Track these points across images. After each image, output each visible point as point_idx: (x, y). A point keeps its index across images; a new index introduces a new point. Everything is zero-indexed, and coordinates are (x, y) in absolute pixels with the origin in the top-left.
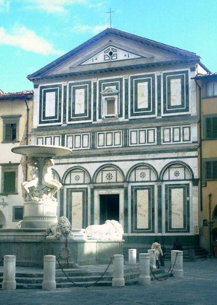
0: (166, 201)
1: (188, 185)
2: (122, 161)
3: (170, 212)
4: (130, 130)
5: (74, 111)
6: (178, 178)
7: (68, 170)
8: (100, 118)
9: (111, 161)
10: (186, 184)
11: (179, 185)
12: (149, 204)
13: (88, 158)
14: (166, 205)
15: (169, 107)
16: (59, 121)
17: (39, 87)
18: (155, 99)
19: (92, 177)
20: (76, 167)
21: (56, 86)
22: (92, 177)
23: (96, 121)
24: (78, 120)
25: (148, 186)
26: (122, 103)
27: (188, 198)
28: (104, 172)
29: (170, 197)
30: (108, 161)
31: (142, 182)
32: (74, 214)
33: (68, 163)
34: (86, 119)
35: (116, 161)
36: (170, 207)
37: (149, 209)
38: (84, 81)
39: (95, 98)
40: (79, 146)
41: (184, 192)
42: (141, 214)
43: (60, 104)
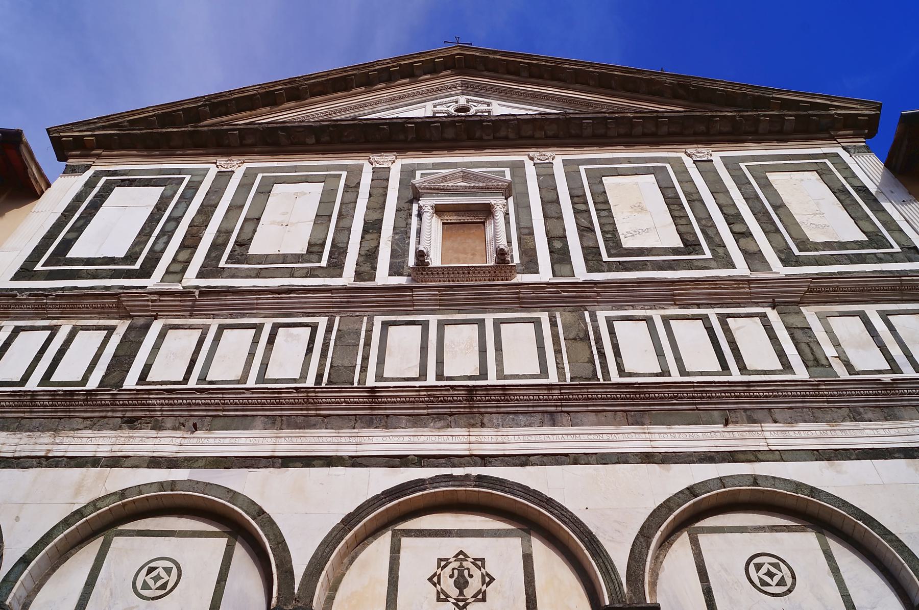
2: (575, 459)
4: (601, 316)
5: (243, 244)
7: (94, 504)
8: (395, 271)
13: (286, 432)
15: (804, 244)
16: (146, 272)
17: (89, 173)
19: (299, 570)
20: (173, 484)
21: (180, 171)
22: (299, 570)
23: (373, 278)
24: (259, 274)
28: (405, 541)
33: (115, 462)
34: (311, 273)
35: (524, 460)
40: (236, 374)
43: (175, 220)
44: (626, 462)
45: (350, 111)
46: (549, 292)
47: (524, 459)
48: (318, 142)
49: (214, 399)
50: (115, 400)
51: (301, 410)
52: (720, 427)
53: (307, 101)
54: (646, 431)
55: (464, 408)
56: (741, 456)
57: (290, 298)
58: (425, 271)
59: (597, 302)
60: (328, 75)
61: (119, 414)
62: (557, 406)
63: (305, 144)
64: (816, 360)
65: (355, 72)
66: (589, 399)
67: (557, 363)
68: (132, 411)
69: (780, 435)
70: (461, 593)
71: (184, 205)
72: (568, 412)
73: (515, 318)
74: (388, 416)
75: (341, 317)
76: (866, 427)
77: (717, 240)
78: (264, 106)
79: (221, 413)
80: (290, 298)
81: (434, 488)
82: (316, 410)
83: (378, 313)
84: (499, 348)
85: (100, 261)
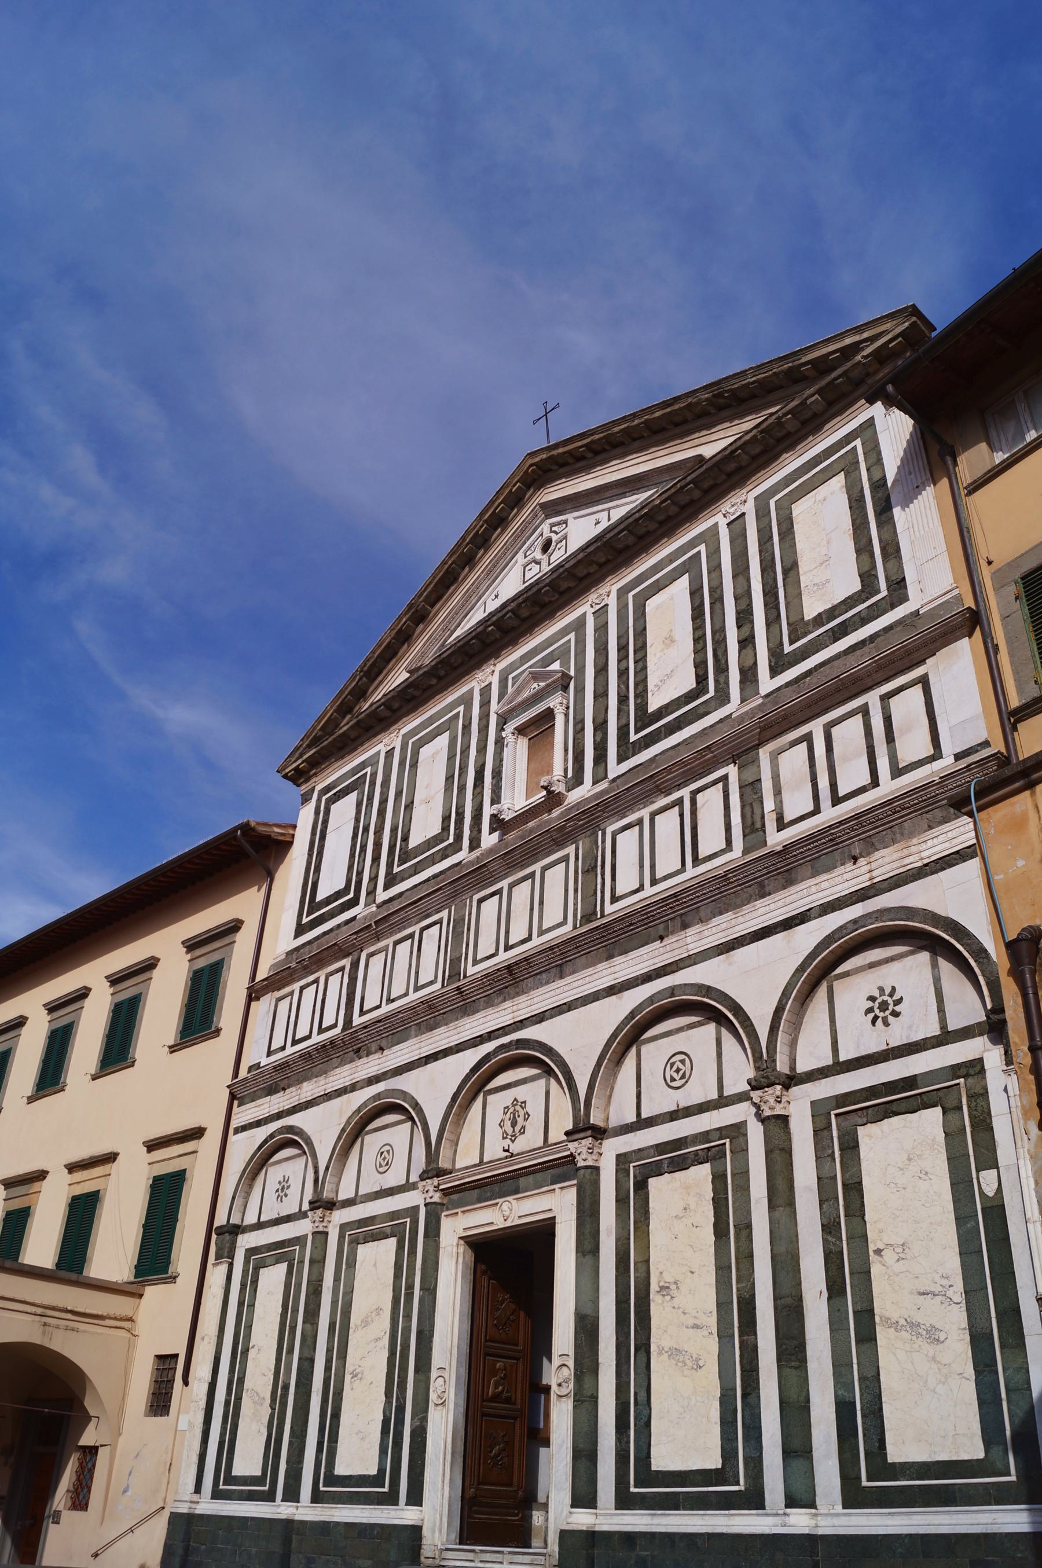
0: (830, 1228)
1: (975, 1068)
3: (866, 1316)
6: (898, 1034)
9: (521, 1024)
10: (955, 1070)
11: (910, 1082)
12: (722, 1269)
14: (832, 1260)
18: (723, 629)
25: (704, 1136)
26: (582, 721)
27: (988, 1181)
29: (855, 1189)
30: (504, 1031)
31: (673, 1116)
32: (354, 1376)
35: (539, 1018)
36: (863, 1275)
37: (723, 1306)
38: (450, 699)
39: (482, 749)
41: (953, 1136)
42: (675, 1353)
44: (598, 1000)
45: (461, 611)
46: (570, 826)
47: (541, 1015)
48: (440, 678)
49: (387, 1023)
50: (344, 1042)
51: (430, 1014)
52: (657, 944)
53: (431, 615)
54: (612, 965)
55: (511, 980)
56: (669, 969)
57: (422, 904)
58: (504, 824)
59: (607, 817)
60: (434, 578)
61: (351, 1049)
62: (562, 959)
63: (432, 686)
64: (753, 824)
65: (452, 559)
66: (577, 947)
67: (574, 904)
68: (355, 1045)
69: (697, 937)
70: (514, 1131)
71: (369, 807)
72: (570, 961)
73: (554, 861)
74: (474, 1001)
75: (455, 905)
76: (761, 905)
77: (723, 662)
78: (403, 644)
79: (395, 1031)
80: (422, 904)
81: (495, 1057)
82: (438, 1011)
83: (474, 891)
84: (541, 903)
85: (332, 899)
